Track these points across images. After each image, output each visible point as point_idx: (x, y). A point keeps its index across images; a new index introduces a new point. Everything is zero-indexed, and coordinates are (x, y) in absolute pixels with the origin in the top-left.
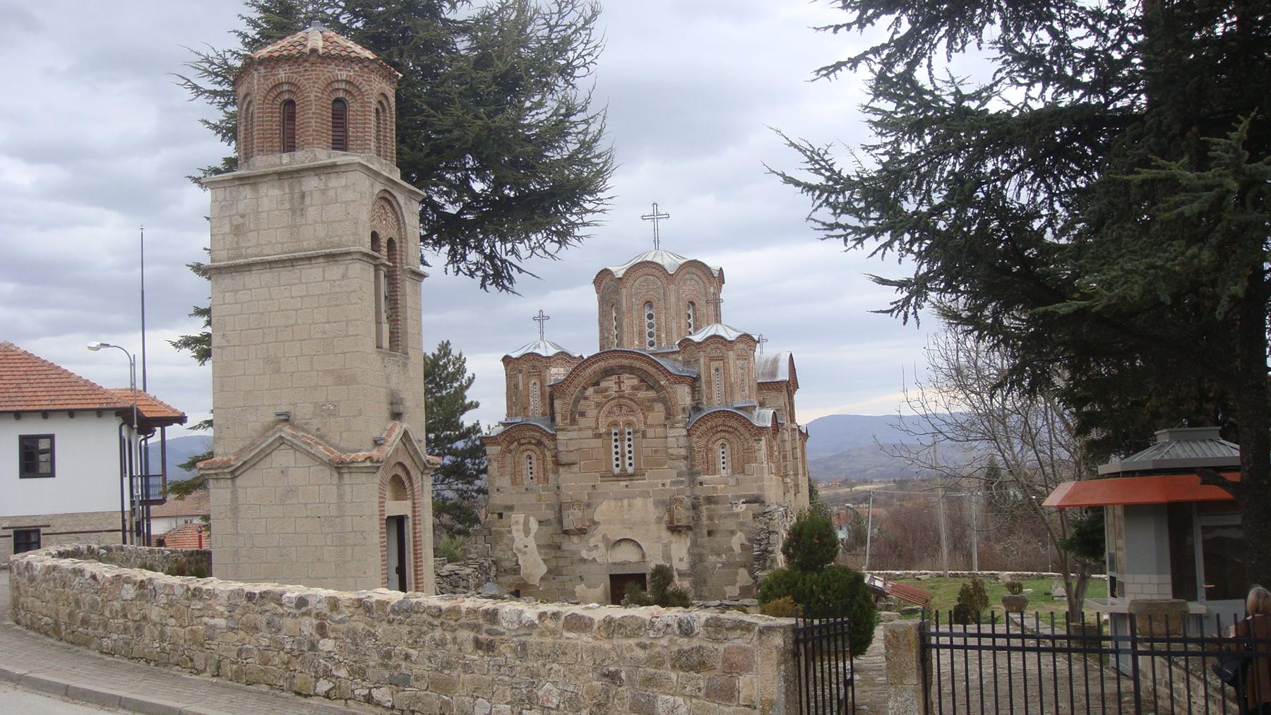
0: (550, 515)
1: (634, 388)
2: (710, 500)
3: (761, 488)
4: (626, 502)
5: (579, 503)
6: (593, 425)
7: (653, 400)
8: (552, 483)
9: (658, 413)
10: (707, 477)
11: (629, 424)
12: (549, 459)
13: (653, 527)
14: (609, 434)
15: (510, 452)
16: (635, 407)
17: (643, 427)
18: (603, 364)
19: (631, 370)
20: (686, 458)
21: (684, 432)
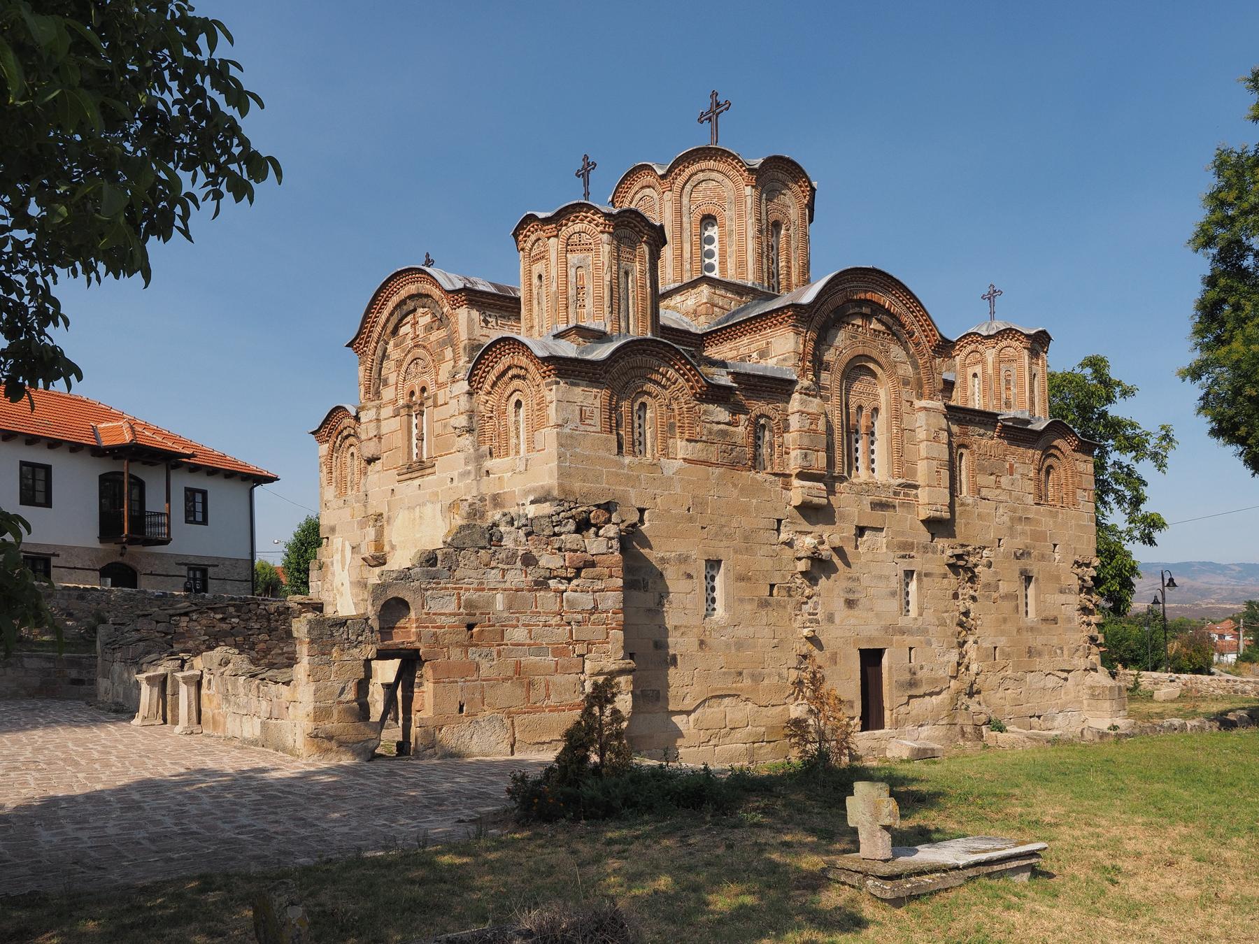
1: (429, 328)
4: (417, 509)
8: (362, 489)
14: (409, 407)
18: (395, 299)
21: (464, 386)
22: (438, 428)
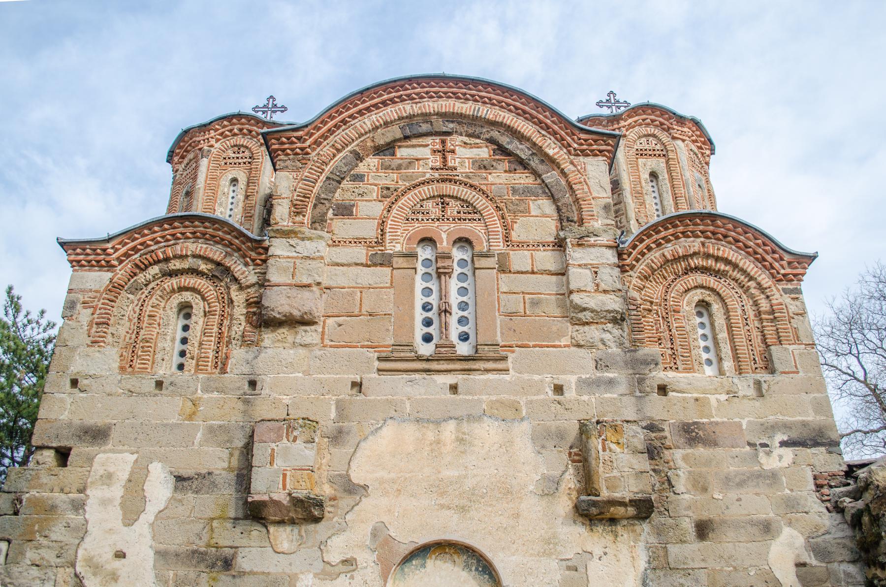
0: (218, 461)
2: (691, 434)
3: (823, 407)
4: (449, 430)
5: (310, 423)
6: (370, 231)
7: (527, 191)
9: (539, 221)
10: (671, 374)
11: (464, 241)
12: (240, 311)
13: (532, 507)
15: (135, 289)
16: (481, 202)
17: (499, 246)
18: (408, 108)
19: (472, 125)
20: (618, 320)
21: (610, 257)
22: (516, 303)
